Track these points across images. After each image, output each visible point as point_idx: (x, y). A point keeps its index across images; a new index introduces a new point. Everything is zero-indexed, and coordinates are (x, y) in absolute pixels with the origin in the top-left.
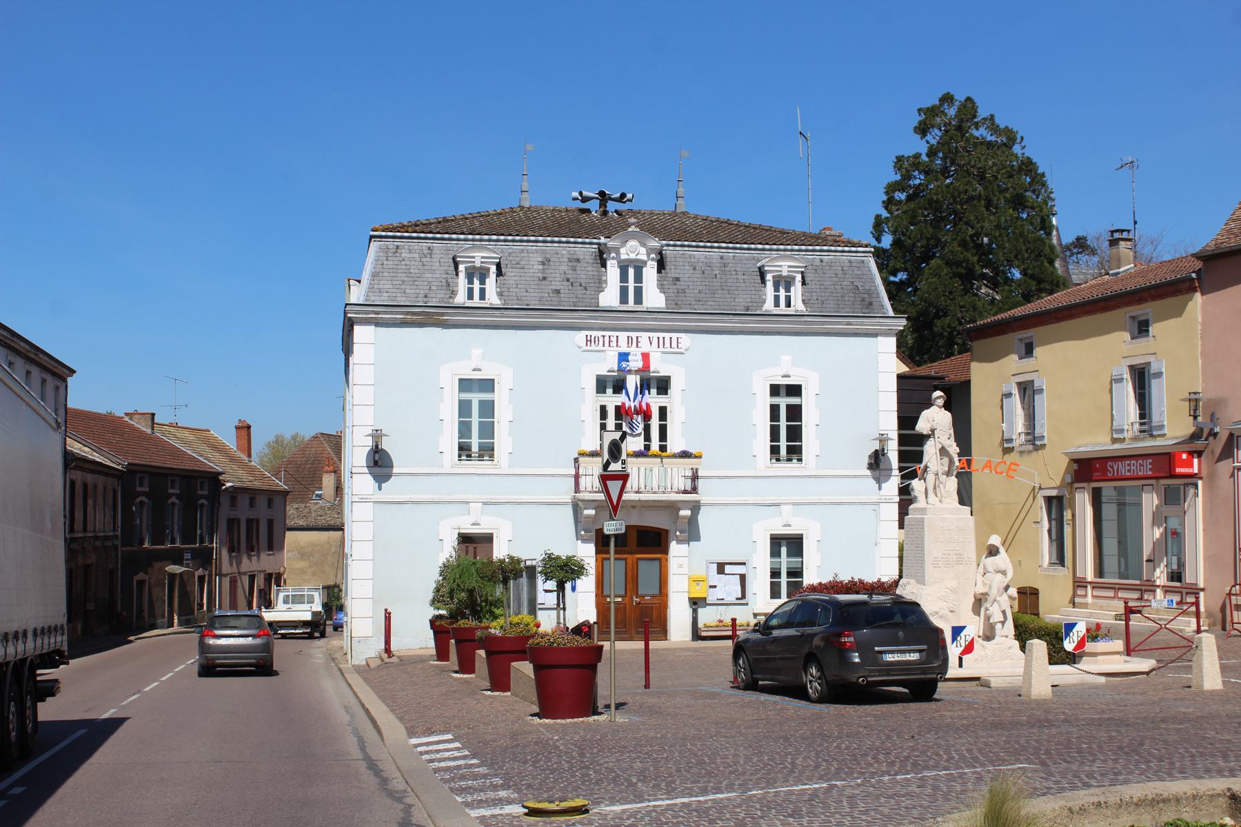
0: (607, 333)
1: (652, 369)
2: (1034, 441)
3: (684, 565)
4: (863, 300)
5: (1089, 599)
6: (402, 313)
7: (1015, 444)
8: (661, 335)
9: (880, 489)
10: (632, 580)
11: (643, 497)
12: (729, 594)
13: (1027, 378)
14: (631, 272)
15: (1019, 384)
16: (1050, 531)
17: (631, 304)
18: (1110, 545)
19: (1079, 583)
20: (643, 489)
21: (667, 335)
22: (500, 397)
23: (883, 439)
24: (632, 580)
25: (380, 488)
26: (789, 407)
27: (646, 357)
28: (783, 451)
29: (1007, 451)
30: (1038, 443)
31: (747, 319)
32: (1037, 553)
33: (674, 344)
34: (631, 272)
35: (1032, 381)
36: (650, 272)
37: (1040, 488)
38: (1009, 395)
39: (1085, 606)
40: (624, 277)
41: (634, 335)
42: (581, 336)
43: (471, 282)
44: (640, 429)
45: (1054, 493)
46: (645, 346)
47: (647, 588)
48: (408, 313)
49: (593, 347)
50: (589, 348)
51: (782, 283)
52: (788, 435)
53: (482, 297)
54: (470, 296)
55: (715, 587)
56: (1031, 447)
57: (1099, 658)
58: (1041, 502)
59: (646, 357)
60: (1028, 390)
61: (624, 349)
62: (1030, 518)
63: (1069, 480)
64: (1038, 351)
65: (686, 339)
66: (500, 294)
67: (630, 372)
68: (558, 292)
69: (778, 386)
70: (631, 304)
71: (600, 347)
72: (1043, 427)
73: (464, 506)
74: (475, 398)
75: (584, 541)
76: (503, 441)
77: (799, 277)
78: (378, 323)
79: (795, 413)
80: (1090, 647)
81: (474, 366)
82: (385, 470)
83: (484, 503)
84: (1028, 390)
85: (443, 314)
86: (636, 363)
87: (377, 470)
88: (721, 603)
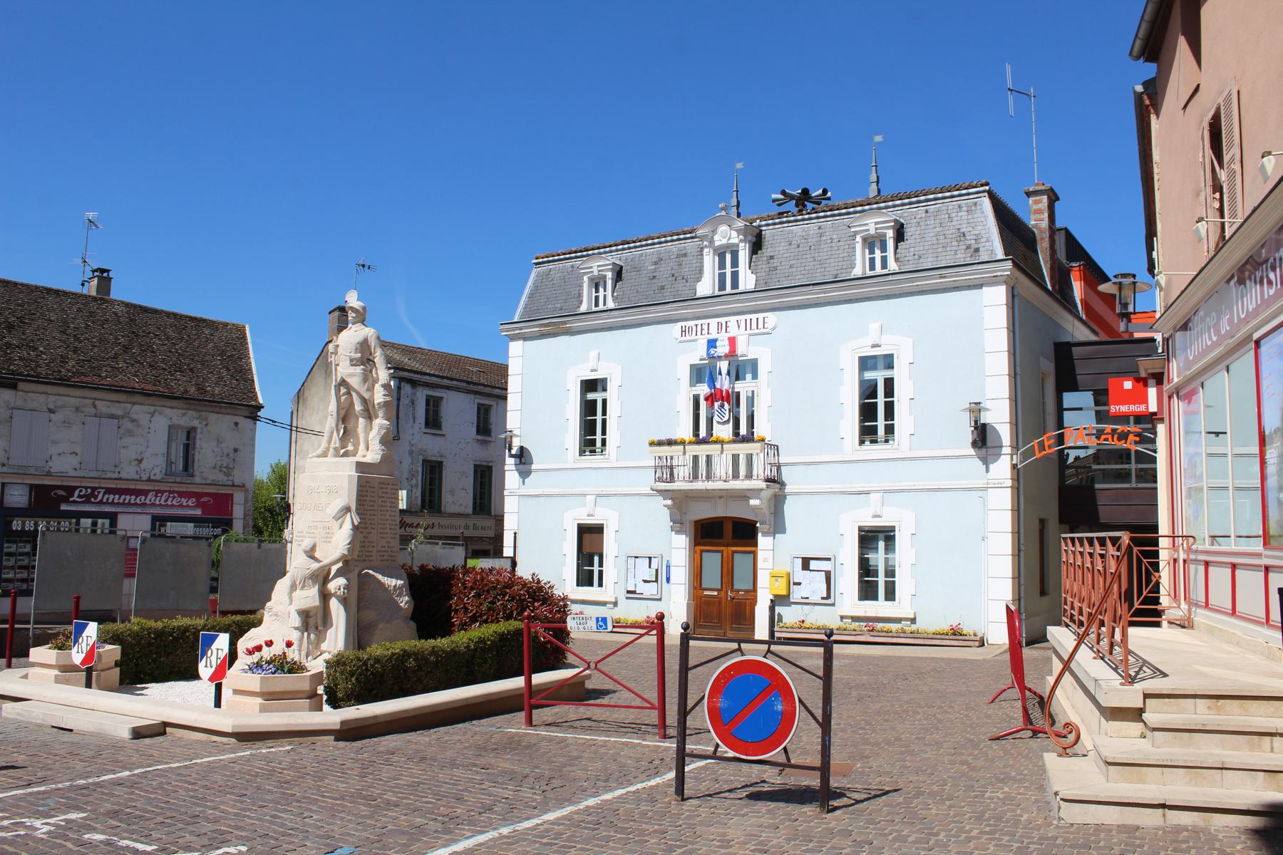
1: (739, 352)
3: (773, 557)
4: (968, 247)
8: (748, 317)
9: (987, 471)
10: (728, 574)
12: (814, 592)
14: (728, 257)
21: (754, 316)
22: (612, 394)
24: (728, 574)
27: (732, 341)
31: (835, 288)
33: (761, 325)
34: (728, 257)
36: (744, 255)
40: (722, 265)
41: (723, 320)
43: (597, 291)
46: (733, 331)
47: (741, 584)
48: (541, 325)
49: (688, 338)
51: (878, 244)
52: (874, 414)
55: (799, 584)
59: (732, 341)
65: (772, 318)
66: (615, 299)
70: (728, 289)
71: (693, 337)
75: (678, 532)
77: (890, 234)
78: (526, 338)
83: (598, 496)
85: (565, 323)
86: (723, 349)
88: (805, 602)
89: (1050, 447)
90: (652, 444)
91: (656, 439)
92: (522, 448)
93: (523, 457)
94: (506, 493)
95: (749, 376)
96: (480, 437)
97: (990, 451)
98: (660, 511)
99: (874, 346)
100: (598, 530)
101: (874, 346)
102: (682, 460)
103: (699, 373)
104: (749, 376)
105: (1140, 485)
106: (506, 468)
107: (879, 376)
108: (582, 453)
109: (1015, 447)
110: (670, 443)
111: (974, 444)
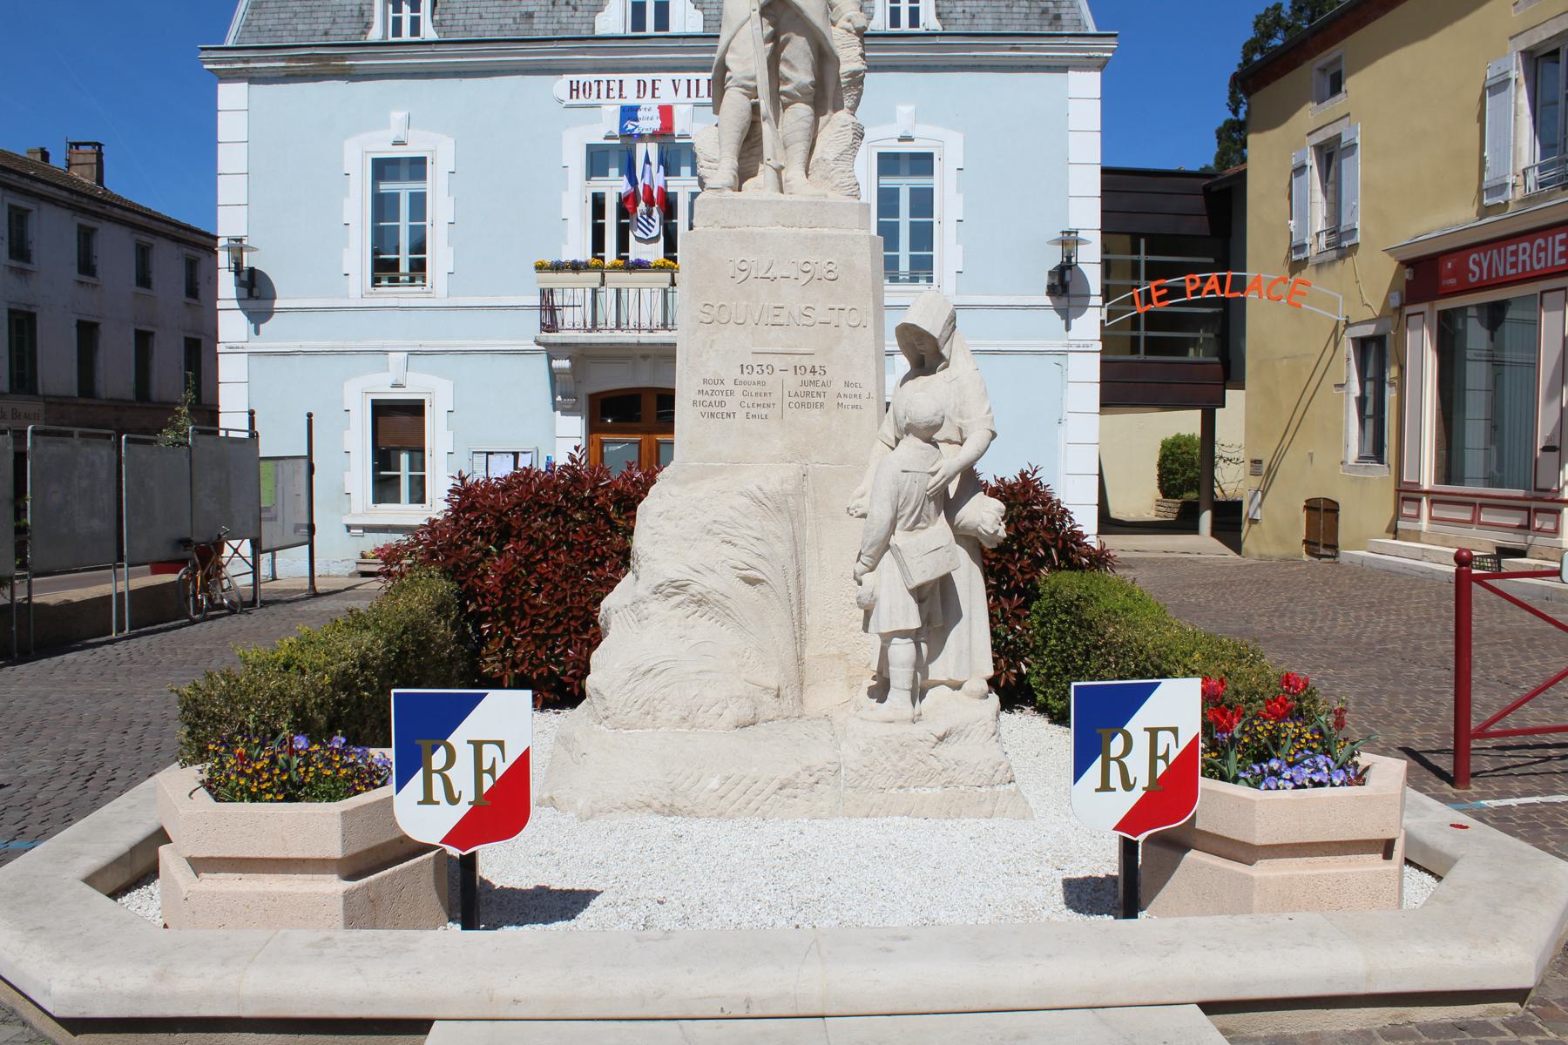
0: (604, 77)
2: (1341, 243)
4: (1045, 11)
5: (1424, 524)
6: (283, 59)
7: (1311, 252)
8: (693, 76)
11: (645, 337)
13: (1330, 132)
15: (1319, 148)
16: (1362, 402)
17: (650, 29)
18: (1475, 432)
19: (1407, 494)
20: (645, 323)
22: (436, 186)
23: (1069, 241)
25: (257, 332)
26: (914, 192)
27: (666, 112)
28: (904, 266)
29: (1297, 267)
30: (1346, 244)
32: (1340, 440)
35: (1338, 138)
37: (1348, 325)
38: (1300, 170)
39: (1416, 536)
41: (648, 77)
42: (561, 84)
44: (657, 229)
45: (1369, 330)
46: (666, 96)
48: (291, 58)
49: (582, 100)
50: (574, 101)
53: (415, 29)
54: (397, 31)
56: (1334, 254)
57: (1263, 870)
58: (1347, 348)
59: (666, 112)
60: (1331, 154)
61: (631, 99)
62: (1329, 381)
63: (1396, 302)
64: (1349, 84)
66: (438, 25)
67: (641, 137)
68: (530, 16)
69: (896, 156)
70: (650, 29)
71: (593, 100)
72: (1356, 217)
73: (382, 357)
74: (403, 189)
75: (565, 412)
76: (438, 257)
78: (253, 78)
79: (923, 202)
80: (1220, 802)
81: (393, 138)
82: (263, 304)
83: (411, 353)
84: (1331, 154)
85: (343, 57)
86: (649, 122)
87: (253, 304)
89: (1160, 299)
90: (540, 268)
91: (548, 261)
92: (252, 270)
93: (255, 288)
94: (220, 348)
95: (686, 170)
96: (15, 263)
97: (1074, 301)
98: (536, 373)
99: (902, 139)
100: (415, 409)
101: (902, 139)
102: (573, 292)
103: (597, 160)
104: (686, 170)
105: (1150, 358)
106: (219, 305)
107: (904, 185)
108: (376, 281)
109: (1107, 293)
110: (558, 267)
111: (1052, 290)
